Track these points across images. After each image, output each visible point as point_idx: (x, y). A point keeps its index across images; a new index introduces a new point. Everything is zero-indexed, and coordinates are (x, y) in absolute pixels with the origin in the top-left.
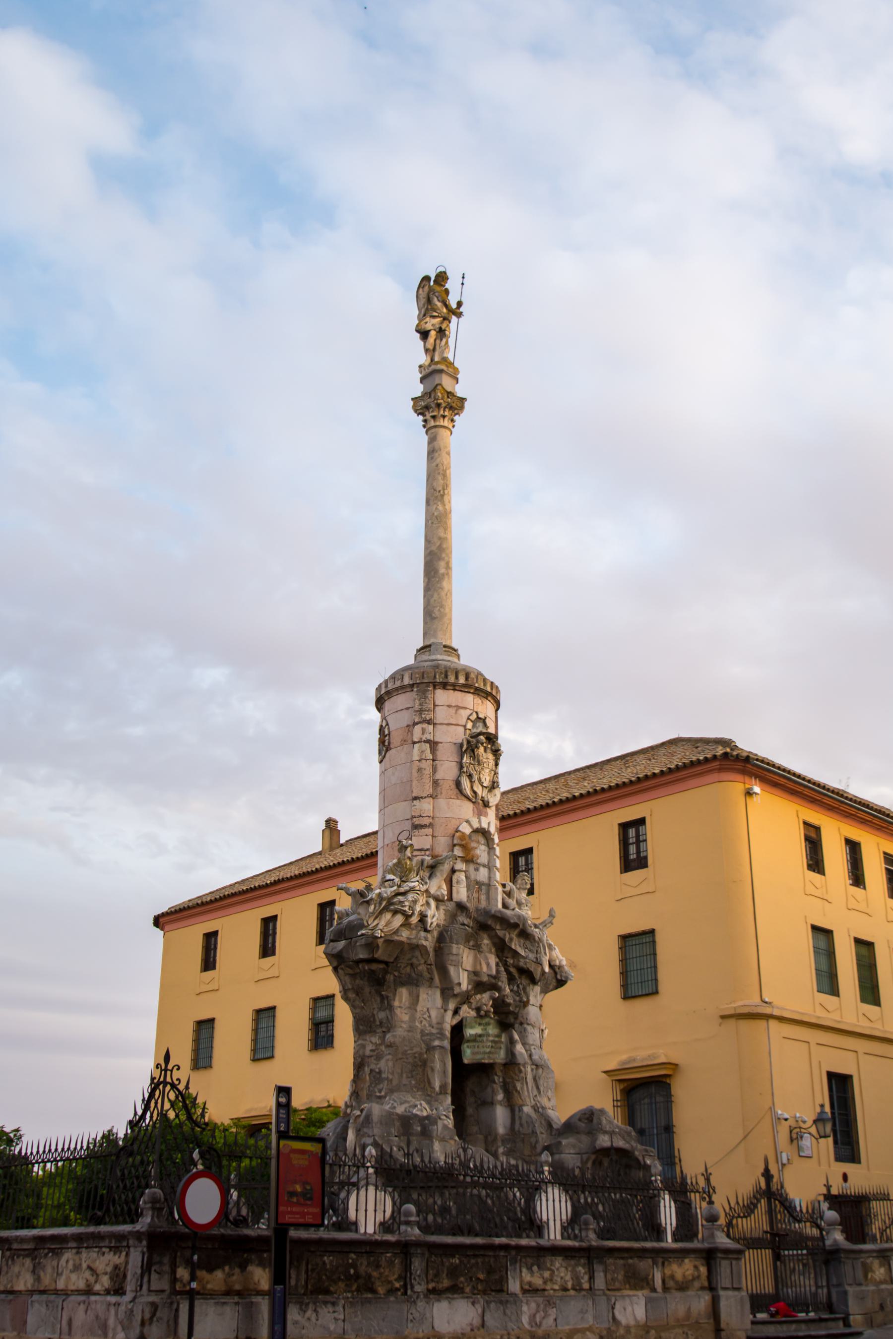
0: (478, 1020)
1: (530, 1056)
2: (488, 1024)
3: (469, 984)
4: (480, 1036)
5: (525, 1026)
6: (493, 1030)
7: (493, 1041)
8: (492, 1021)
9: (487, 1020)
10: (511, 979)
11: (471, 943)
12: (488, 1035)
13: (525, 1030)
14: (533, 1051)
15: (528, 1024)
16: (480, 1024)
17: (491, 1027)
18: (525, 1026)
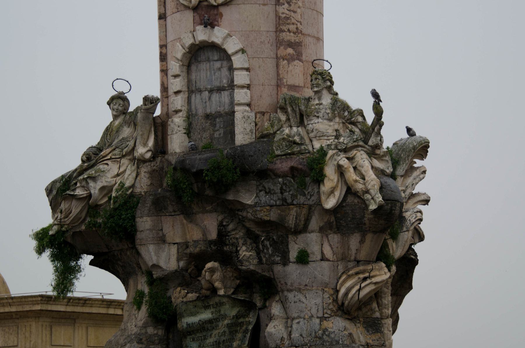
0: (199, 304)
1: (290, 334)
2: (221, 304)
3: (178, 260)
4: (210, 321)
5: (286, 293)
6: (231, 311)
7: (228, 326)
8: (225, 300)
9: (217, 299)
10: (252, 237)
11: (170, 209)
12: (224, 317)
13: (286, 298)
14: (295, 326)
15: (290, 291)
16: (206, 307)
17: (227, 306)
18: (286, 293)
